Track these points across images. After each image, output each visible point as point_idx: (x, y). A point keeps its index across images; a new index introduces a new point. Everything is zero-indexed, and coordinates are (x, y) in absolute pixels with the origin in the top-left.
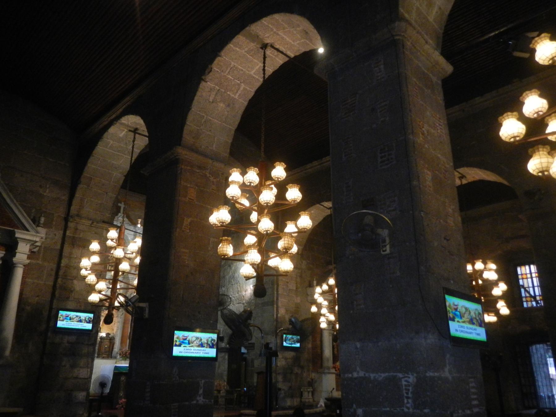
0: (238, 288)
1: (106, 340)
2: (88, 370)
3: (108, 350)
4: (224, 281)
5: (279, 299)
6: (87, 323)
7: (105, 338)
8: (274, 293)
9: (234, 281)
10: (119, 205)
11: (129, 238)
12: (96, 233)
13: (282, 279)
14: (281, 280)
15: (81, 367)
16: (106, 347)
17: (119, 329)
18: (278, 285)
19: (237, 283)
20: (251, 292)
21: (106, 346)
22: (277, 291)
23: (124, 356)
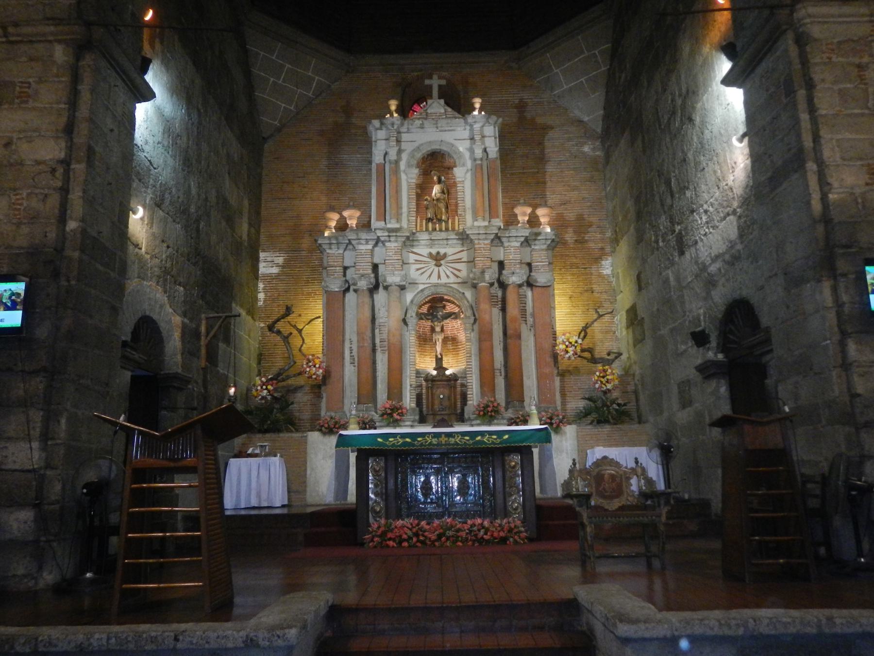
0: (715, 172)
1: (439, 383)
2: (31, 448)
3: (446, 403)
4: (687, 170)
5: (824, 133)
6: (7, 308)
7: (437, 379)
8: (797, 121)
9: (704, 156)
10: (427, 82)
11: (461, 149)
12: (31, 59)
13: (830, 58)
14: (825, 64)
15: (9, 439)
16: (441, 399)
17: (473, 356)
18: (810, 86)
19: (711, 160)
20: (746, 164)
21: (441, 396)
22: (812, 109)
23: (482, 413)
